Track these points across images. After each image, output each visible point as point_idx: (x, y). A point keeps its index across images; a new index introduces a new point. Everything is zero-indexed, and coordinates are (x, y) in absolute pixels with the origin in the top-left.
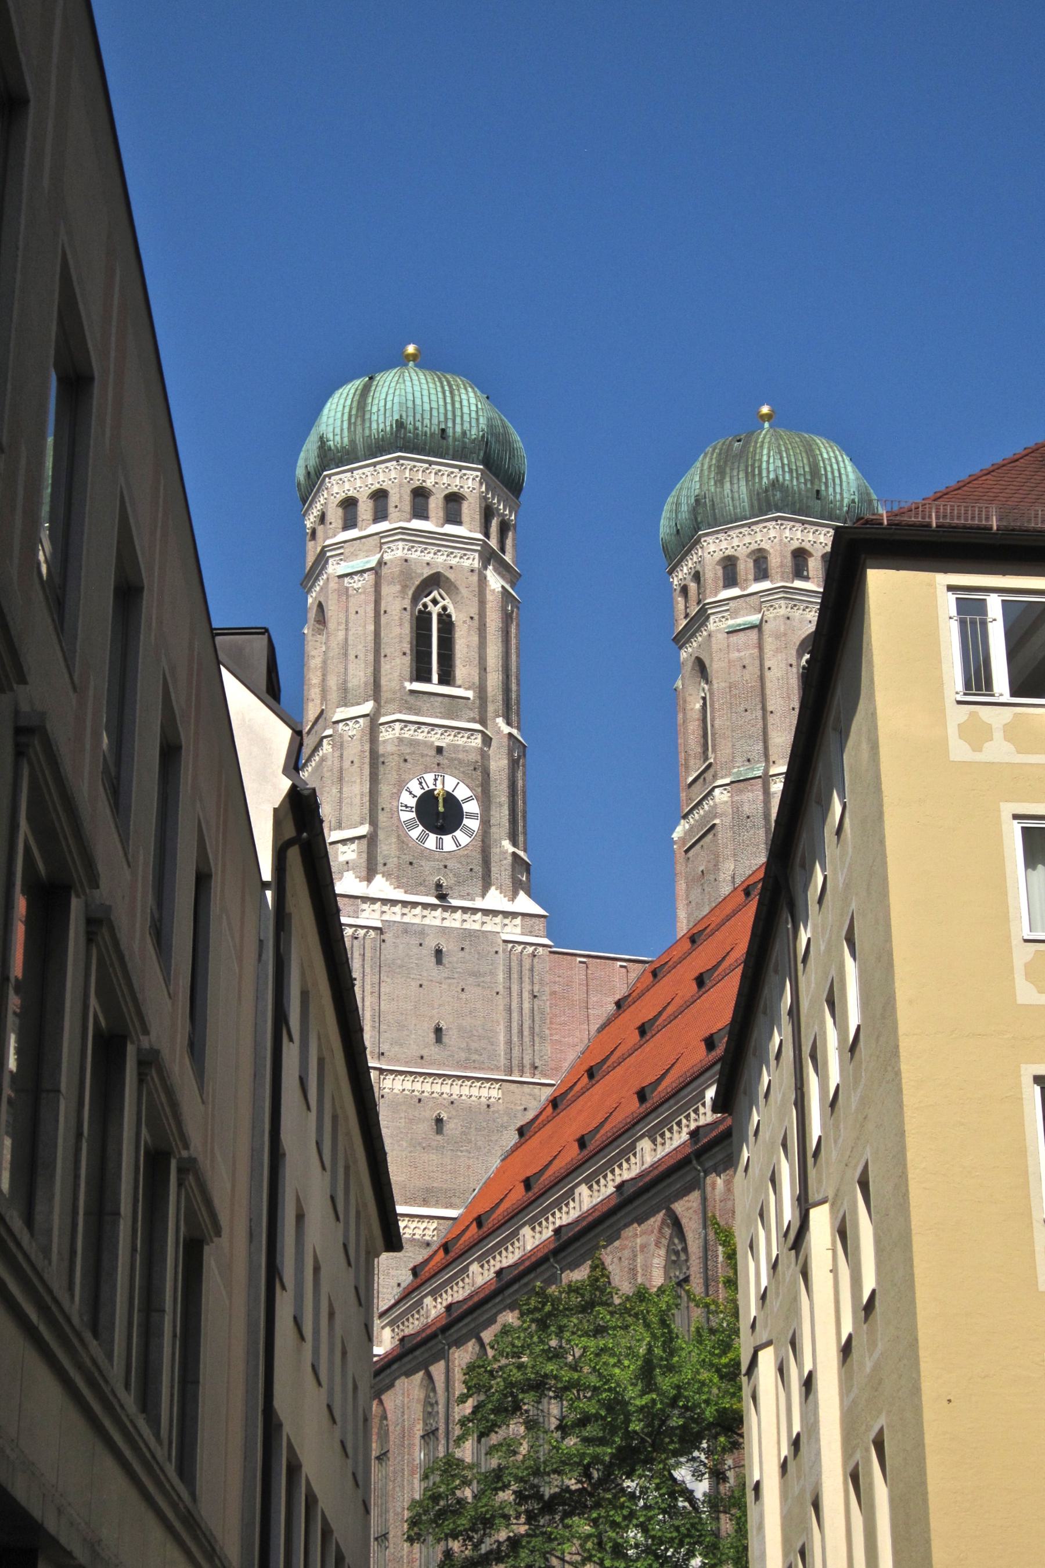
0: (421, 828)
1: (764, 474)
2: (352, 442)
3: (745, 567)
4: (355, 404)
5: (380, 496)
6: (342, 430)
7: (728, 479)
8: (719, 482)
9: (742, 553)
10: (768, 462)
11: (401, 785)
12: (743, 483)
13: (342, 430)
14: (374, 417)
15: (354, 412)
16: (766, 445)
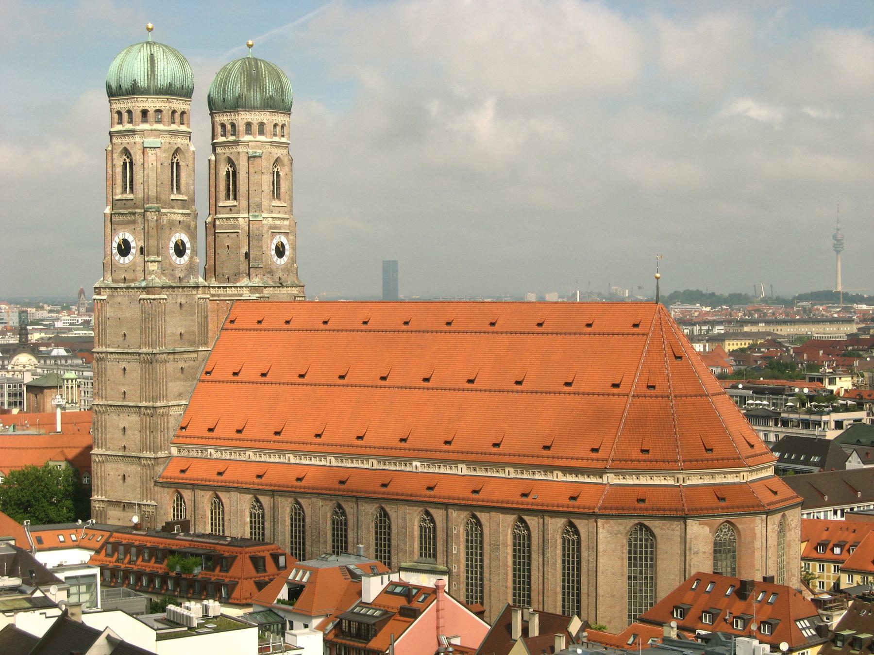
0: (175, 256)
1: (268, 92)
2: (149, 86)
3: (255, 128)
4: (149, 69)
5: (159, 111)
6: (144, 80)
7: (252, 90)
8: (249, 90)
9: (255, 122)
10: (269, 86)
11: (169, 239)
12: (258, 93)
13: (144, 80)
14: (159, 78)
15: (149, 73)
16: (267, 78)
